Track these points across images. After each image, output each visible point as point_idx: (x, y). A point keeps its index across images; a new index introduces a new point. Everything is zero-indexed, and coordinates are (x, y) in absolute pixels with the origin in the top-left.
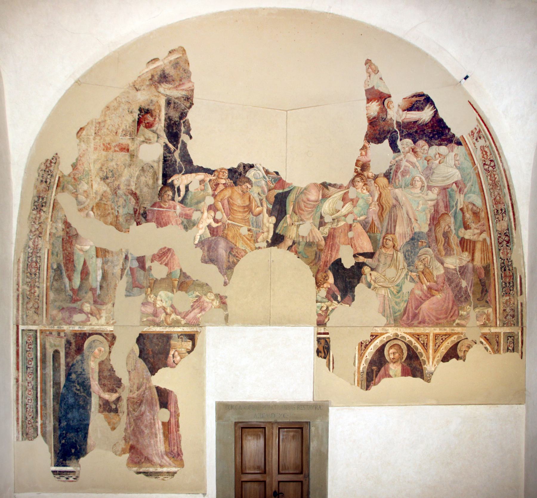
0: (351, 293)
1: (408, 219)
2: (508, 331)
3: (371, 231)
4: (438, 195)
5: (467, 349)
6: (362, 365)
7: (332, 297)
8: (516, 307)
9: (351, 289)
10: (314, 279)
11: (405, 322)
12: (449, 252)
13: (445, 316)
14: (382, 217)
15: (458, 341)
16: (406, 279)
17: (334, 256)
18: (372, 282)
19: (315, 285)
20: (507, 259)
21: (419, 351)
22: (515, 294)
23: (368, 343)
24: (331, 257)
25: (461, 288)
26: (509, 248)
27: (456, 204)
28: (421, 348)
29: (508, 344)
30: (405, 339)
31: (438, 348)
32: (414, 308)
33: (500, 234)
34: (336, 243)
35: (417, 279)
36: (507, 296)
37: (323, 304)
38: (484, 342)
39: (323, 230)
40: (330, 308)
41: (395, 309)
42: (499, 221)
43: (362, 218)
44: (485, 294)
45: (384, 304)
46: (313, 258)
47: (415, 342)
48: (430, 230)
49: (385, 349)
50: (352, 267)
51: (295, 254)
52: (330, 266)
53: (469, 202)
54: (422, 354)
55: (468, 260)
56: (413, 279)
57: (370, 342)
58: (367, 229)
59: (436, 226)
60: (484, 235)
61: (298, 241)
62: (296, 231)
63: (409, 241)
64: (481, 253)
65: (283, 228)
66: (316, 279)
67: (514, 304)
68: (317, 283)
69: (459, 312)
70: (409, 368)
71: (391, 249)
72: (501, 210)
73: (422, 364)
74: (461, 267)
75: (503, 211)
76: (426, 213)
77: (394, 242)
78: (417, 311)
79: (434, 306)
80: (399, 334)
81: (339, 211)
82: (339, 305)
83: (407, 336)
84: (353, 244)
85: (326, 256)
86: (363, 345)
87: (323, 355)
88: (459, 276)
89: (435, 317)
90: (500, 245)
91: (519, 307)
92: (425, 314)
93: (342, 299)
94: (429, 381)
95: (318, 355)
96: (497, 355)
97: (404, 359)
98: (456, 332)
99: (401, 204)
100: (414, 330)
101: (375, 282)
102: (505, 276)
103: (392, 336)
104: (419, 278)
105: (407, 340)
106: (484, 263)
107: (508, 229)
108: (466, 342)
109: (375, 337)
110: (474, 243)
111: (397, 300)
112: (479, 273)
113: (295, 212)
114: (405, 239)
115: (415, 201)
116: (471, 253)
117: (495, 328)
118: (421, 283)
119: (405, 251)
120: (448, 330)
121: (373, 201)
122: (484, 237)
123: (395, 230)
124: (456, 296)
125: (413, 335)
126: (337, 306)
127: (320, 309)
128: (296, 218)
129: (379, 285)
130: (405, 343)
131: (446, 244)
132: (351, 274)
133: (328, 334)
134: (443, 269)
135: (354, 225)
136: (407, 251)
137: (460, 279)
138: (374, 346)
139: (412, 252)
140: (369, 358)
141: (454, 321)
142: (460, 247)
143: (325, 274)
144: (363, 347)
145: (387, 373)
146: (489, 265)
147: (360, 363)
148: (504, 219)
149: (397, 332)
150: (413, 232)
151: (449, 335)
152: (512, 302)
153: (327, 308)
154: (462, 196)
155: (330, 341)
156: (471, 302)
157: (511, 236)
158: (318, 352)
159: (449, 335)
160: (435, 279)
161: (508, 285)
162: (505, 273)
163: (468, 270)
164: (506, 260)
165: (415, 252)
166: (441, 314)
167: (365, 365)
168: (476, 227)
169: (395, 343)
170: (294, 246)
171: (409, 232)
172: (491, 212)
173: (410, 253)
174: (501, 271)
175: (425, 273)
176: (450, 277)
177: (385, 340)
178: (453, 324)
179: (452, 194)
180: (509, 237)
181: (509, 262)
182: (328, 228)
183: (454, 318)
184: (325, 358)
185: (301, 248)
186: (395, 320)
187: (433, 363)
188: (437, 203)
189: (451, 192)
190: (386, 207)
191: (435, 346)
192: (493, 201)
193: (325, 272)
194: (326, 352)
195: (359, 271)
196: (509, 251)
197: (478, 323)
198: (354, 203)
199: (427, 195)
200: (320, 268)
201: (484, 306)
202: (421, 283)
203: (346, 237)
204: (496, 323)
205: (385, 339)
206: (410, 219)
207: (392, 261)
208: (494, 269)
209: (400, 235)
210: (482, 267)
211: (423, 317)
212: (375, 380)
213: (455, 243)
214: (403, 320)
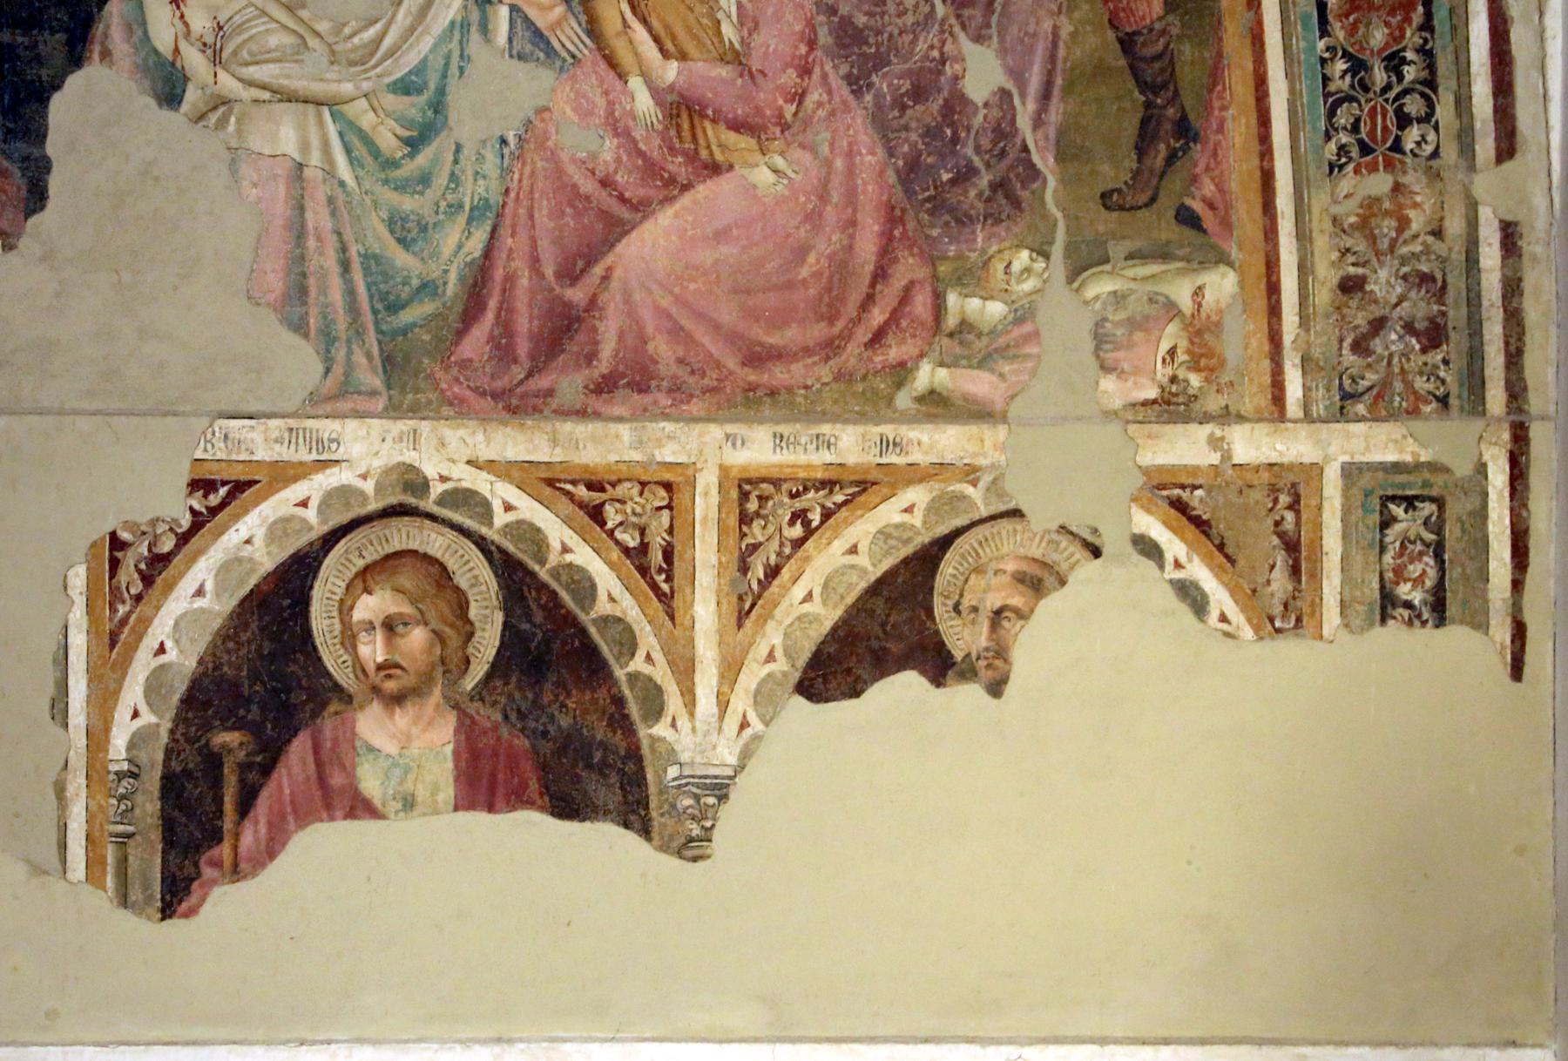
0: (20, 147)
5: (1017, 601)
8: (1458, 256)
13: (819, 331)
15: (942, 530)
16: (475, 36)
18: (195, 61)
21: (603, 607)
22: (1450, 153)
25: (956, 105)
28: (617, 589)
30: (484, 510)
31: (764, 584)
32: (549, 271)
36: (1373, 168)
41: (387, 277)
44: (1172, 158)
45: (300, 234)
47: (572, 539)
49: (318, 593)
54: (629, 630)
56: (537, 34)
67: (1438, 233)
78: (576, 295)
80: (430, 470)
83: (499, 492)
89: (732, 338)
91: (1490, 256)
98: (916, 457)
100: (554, 442)
101: (216, 59)
103: (369, 487)
105: (501, 518)
111: (408, 203)
117: (1262, 429)
118: (612, 63)
124: (911, 171)
125: (550, 482)
129: (250, 83)
130: (481, 543)
137: (945, 31)
138: (224, 570)
141: (901, 372)
149: (410, 457)
152: (1418, 221)
156: (1046, 216)
160: (729, 32)
161: (1379, 76)
166: (779, 320)
176: (861, 20)
178: (890, 400)
183: (894, 352)
186: (392, 364)
187: (723, 705)
191: (744, 568)
197: (1113, 391)
201: (1164, 255)
202: (612, 63)
211: (630, 340)
214: (465, 364)
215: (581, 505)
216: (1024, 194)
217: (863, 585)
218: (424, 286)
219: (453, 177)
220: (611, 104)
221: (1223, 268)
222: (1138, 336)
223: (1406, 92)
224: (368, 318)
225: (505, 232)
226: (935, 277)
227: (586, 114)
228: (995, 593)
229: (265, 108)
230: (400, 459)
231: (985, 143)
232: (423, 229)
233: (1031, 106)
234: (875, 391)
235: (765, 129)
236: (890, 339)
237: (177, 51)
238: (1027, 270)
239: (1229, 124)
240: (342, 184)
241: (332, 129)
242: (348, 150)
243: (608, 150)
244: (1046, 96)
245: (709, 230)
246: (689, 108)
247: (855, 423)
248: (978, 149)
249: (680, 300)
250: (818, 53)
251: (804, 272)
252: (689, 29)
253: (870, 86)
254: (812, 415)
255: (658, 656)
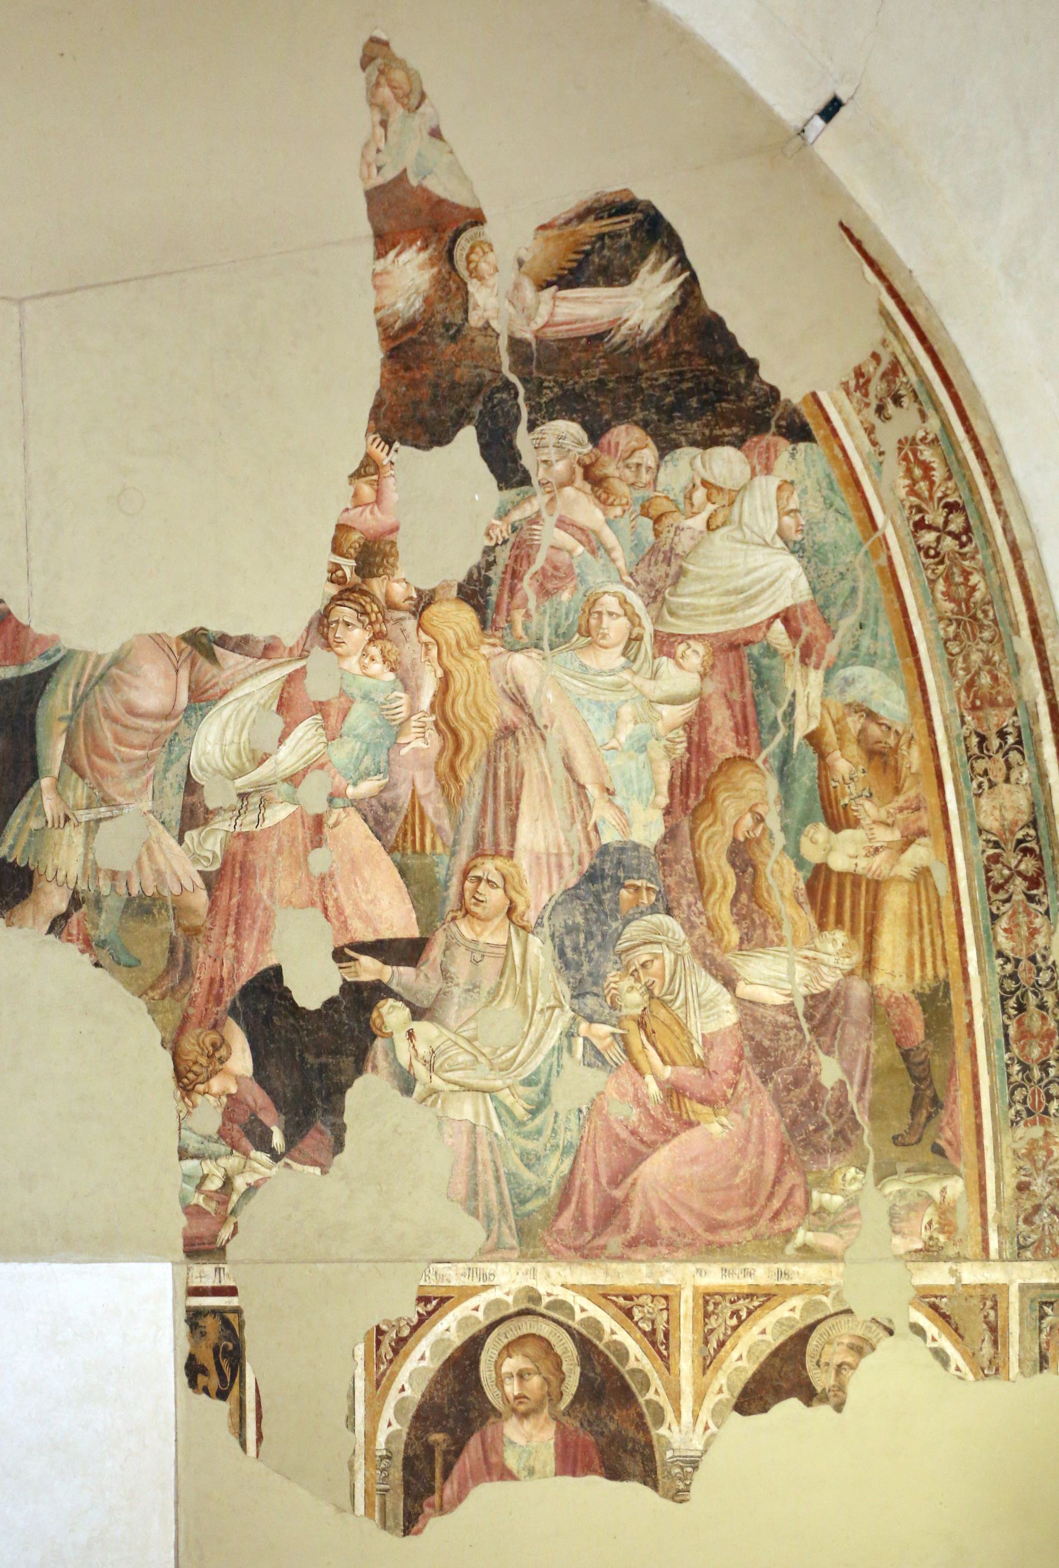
0: (331, 1118)
1: (573, 787)
2: (1044, 1280)
3: (409, 844)
4: (703, 676)
5: (850, 1359)
6: (383, 1425)
7: (248, 1133)
9: (327, 1099)
10: (167, 1056)
11: (569, 1242)
12: (759, 932)
13: (745, 1212)
14: (457, 779)
15: (810, 1321)
16: (565, 1054)
17: (249, 957)
18: (420, 1071)
19: (172, 1084)
20: (1033, 959)
21: (632, 1364)
23: (406, 1332)
24: (238, 960)
25: (817, 1089)
26: (1042, 909)
27: (789, 714)
28: (640, 1354)
29: (1043, 1336)
30: (570, 1311)
31: (717, 1351)
32: (604, 1180)
33: (996, 845)
34: (259, 899)
35: (615, 1053)
36: (1034, 1123)
37: (208, 1166)
38: (931, 1329)
39: (200, 844)
40: (240, 1183)
42: (992, 785)
43: (368, 787)
44: (929, 1118)
45: (474, 1161)
46: (162, 965)
48: (671, 835)
50: (331, 1003)
51: (82, 952)
52: (234, 1002)
53: (849, 705)
54: (646, 1376)
55: (846, 964)
56: (598, 1053)
57: (414, 1329)
58: (391, 836)
59: (695, 816)
60: (920, 853)
61: (91, 895)
62: (81, 850)
63: (577, 887)
64: (910, 935)
65: (25, 836)
66: (176, 1056)
68: (179, 1075)
69: (808, 1194)
70: (591, 1438)
71: (497, 921)
72: (1002, 734)
73: (649, 1420)
74: (813, 996)
75: (1011, 740)
76: (651, 761)
77: (513, 894)
78: (618, 1194)
79: (697, 1169)
80: (542, 1290)
81: (266, 757)
82: (276, 1169)
83: (578, 1301)
84: (330, 903)
85: (217, 959)
86: (386, 1341)
87: (214, 1382)
88: (808, 1038)
89: (699, 1216)
90: (994, 897)
92: (655, 1205)
93: (290, 1141)
94: (679, 1496)
95: (193, 1384)
96: (992, 1386)
97: (567, 1399)
98: (796, 1281)
99: (541, 722)
100: (607, 1274)
101: (431, 1069)
102: (1025, 1035)
103: (510, 1299)
104: (627, 1050)
105: (579, 1316)
106: (923, 977)
107: (1034, 823)
108: (845, 1330)
109: (439, 1305)
110: (876, 887)
111: (530, 1145)
112: (900, 1023)
113: (75, 767)
114: (561, 877)
115: (601, 705)
116: (861, 935)
117: (977, 1265)
118: (637, 1068)
119: (560, 930)
120: (762, 1274)
121: (413, 710)
122: (918, 863)
123: (513, 838)
124: (794, 1125)
125: (605, 1296)
126: (267, 1172)
127: (198, 1188)
128: (79, 792)
129: (449, 1082)
130: (569, 1329)
131: (744, 898)
132: (324, 1034)
133: (232, 1291)
134: (731, 1008)
135: (331, 821)
136: (571, 930)
139: (590, 936)
140: (415, 1394)
141: (788, 1235)
142: (807, 907)
143: (213, 1036)
144: (386, 1349)
145: (494, 1459)
146: (947, 985)
147: (373, 1416)
148: (1014, 776)
149: (531, 1283)
150: (596, 846)
151: (768, 1297)
153: (228, 1182)
154: (816, 677)
155: (242, 1325)
156: (864, 1149)
157: (1047, 853)
158: (193, 1370)
159: (768, 1297)
160: (698, 1050)
161: (1037, 1074)
162: (1020, 1023)
163: (846, 1010)
164: (1025, 963)
165: (604, 936)
166: (724, 1206)
167: (396, 1426)
168: (883, 815)
169: (525, 1330)
170: (75, 917)
171: (576, 847)
172: (950, 748)
173: (582, 936)
174: (1004, 1011)
175: (652, 1024)
176: (766, 1043)
177: (483, 1319)
178: (783, 1250)
179: (771, 668)
180: (1040, 858)
181: (1039, 970)
182: (221, 835)
183: (785, 1223)
184: (222, 1395)
185: (106, 925)
186: (523, 1233)
187: (696, 1417)
188: (702, 709)
189: (765, 661)
190: (472, 734)
191: (706, 1342)
192: (963, 694)
193: (215, 1027)
194: (227, 1372)
195: (359, 1021)
196: (1038, 922)
197: (900, 1244)
198: (332, 721)
199: (654, 676)
200: (191, 1011)
201: (925, 1170)
202: (637, 1068)
203: (301, 874)
204: (985, 1241)
205: (480, 1315)
206: (582, 787)
207: (502, 974)
208: (969, 1003)
209: (538, 858)
210: (912, 997)
211: (646, 1218)
212: (442, 1490)
213: (788, 891)
214: (560, 1232)
215: (621, 1308)
216: (852, 1137)
217: (768, 1351)
218: (538, 1190)
219: (554, 1131)
220: (636, 1090)
221: (956, 1177)
222: (912, 1214)
223: (1050, 1082)
224: (510, 1207)
225: (581, 1160)
226: (806, 1183)
227: (623, 1095)
228: (838, 1355)
229: (457, 1095)
230: (526, 1284)
231: (832, 1109)
232: (538, 1159)
233: (856, 1089)
234: (775, 1246)
235: (716, 1102)
236: (782, 1217)
237: (411, 1065)
238: (854, 1179)
239: (959, 1100)
240: (496, 1135)
241: (491, 1106)
242: (499, 1117)
243: (634, 1115)
244: (863, 1084)
245: (688, 1158)
246: (678, 1093)
247: (764, 1262)
248: (828, 1112)
249: (672, 1196)
250: (744, 1061)
251: (738, 1180)
252: (677, 1049)
253: (772, 1078)
254: (742, 1258)
255: (661, 1390)
